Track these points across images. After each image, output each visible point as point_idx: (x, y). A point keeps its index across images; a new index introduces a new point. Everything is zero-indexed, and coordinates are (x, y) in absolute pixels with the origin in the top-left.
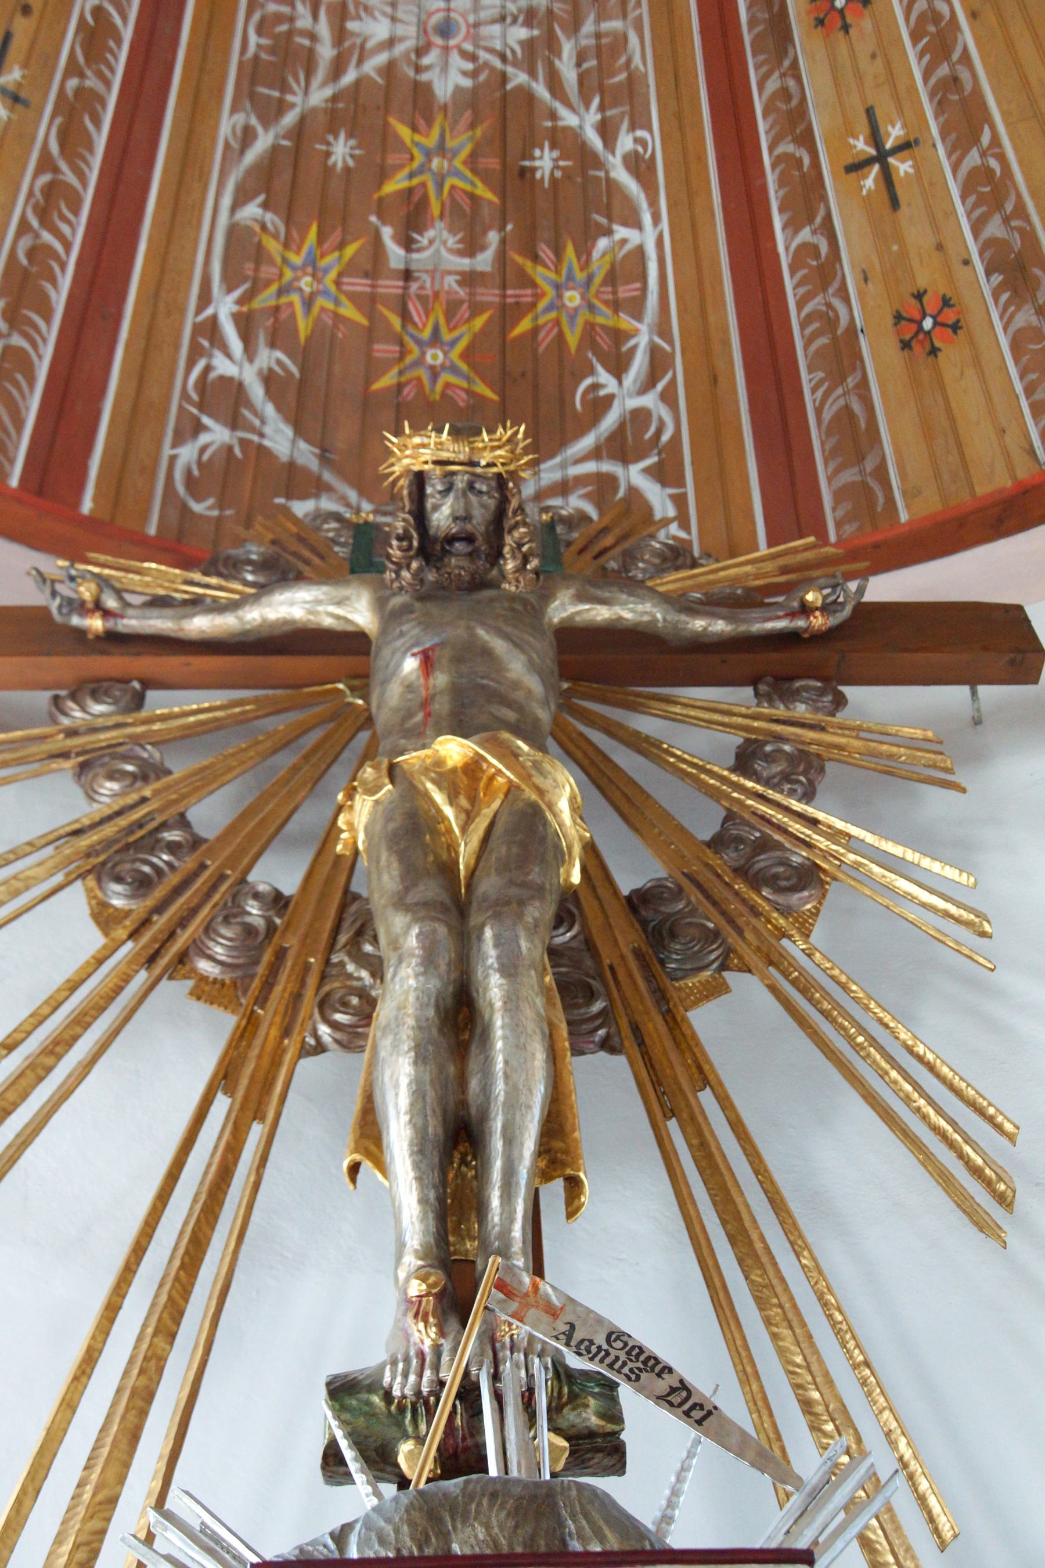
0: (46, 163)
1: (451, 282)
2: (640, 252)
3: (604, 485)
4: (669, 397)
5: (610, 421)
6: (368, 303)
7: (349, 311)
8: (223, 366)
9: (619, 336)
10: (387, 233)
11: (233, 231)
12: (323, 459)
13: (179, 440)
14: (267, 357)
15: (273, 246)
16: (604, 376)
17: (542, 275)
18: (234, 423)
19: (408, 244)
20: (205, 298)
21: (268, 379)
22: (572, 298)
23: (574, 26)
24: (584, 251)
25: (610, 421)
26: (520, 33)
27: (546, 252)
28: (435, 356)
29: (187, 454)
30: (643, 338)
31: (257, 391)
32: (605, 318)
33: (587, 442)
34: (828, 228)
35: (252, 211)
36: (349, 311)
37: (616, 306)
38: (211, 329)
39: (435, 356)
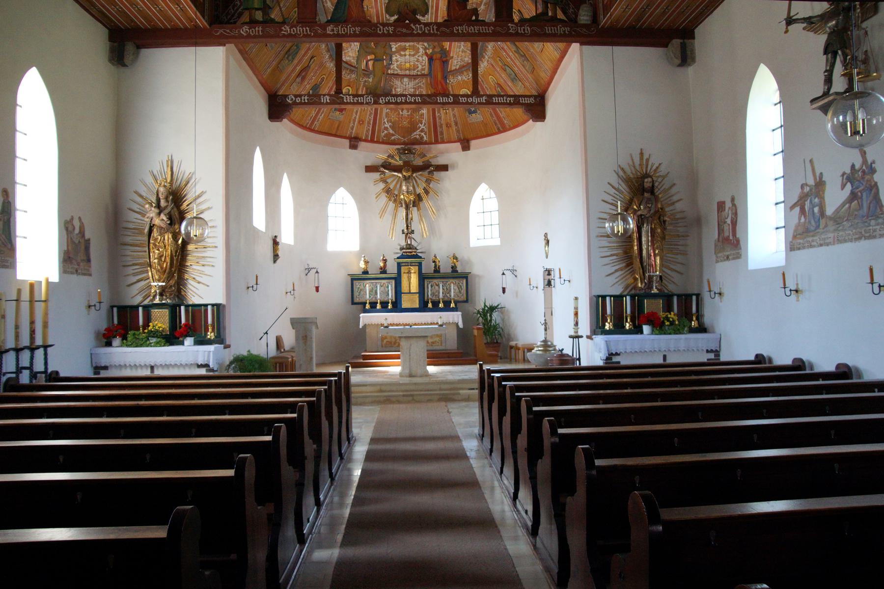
0: (370, 111)
1: (406, 116)
2: (424, 113)
3: (420, 135)
4: (426, 127)
5: (421, 129)
6: (399, 118)
7: (397, 119)
8: (386, 126)
9: (422, 121)
10: (400, 111)
11: (386, 113)
12: (395, 133)
13: (382, 133)
14: (390, 124)
15: (390, 114)
16: (420, 125)
17: (415, 115)
18: (387, 131)
19: (402, 112)
20: (384, 120)
21: (390, 126)
22: (417, 117)
23: (418, 90)
24: (419, 112)
25: (421, 129)
26: (413, 90)
27: (415, 113)
28: (405, 123)
29: (383, 134)
30: (424, 122)
31: (389, 127)
32: (420, 119)
33: (418, 131)
34: (441, 114)
35: (388, 110)
36: (397, 119)
37: (421, 118)
38: (385, 123)
39: (405, 123)
